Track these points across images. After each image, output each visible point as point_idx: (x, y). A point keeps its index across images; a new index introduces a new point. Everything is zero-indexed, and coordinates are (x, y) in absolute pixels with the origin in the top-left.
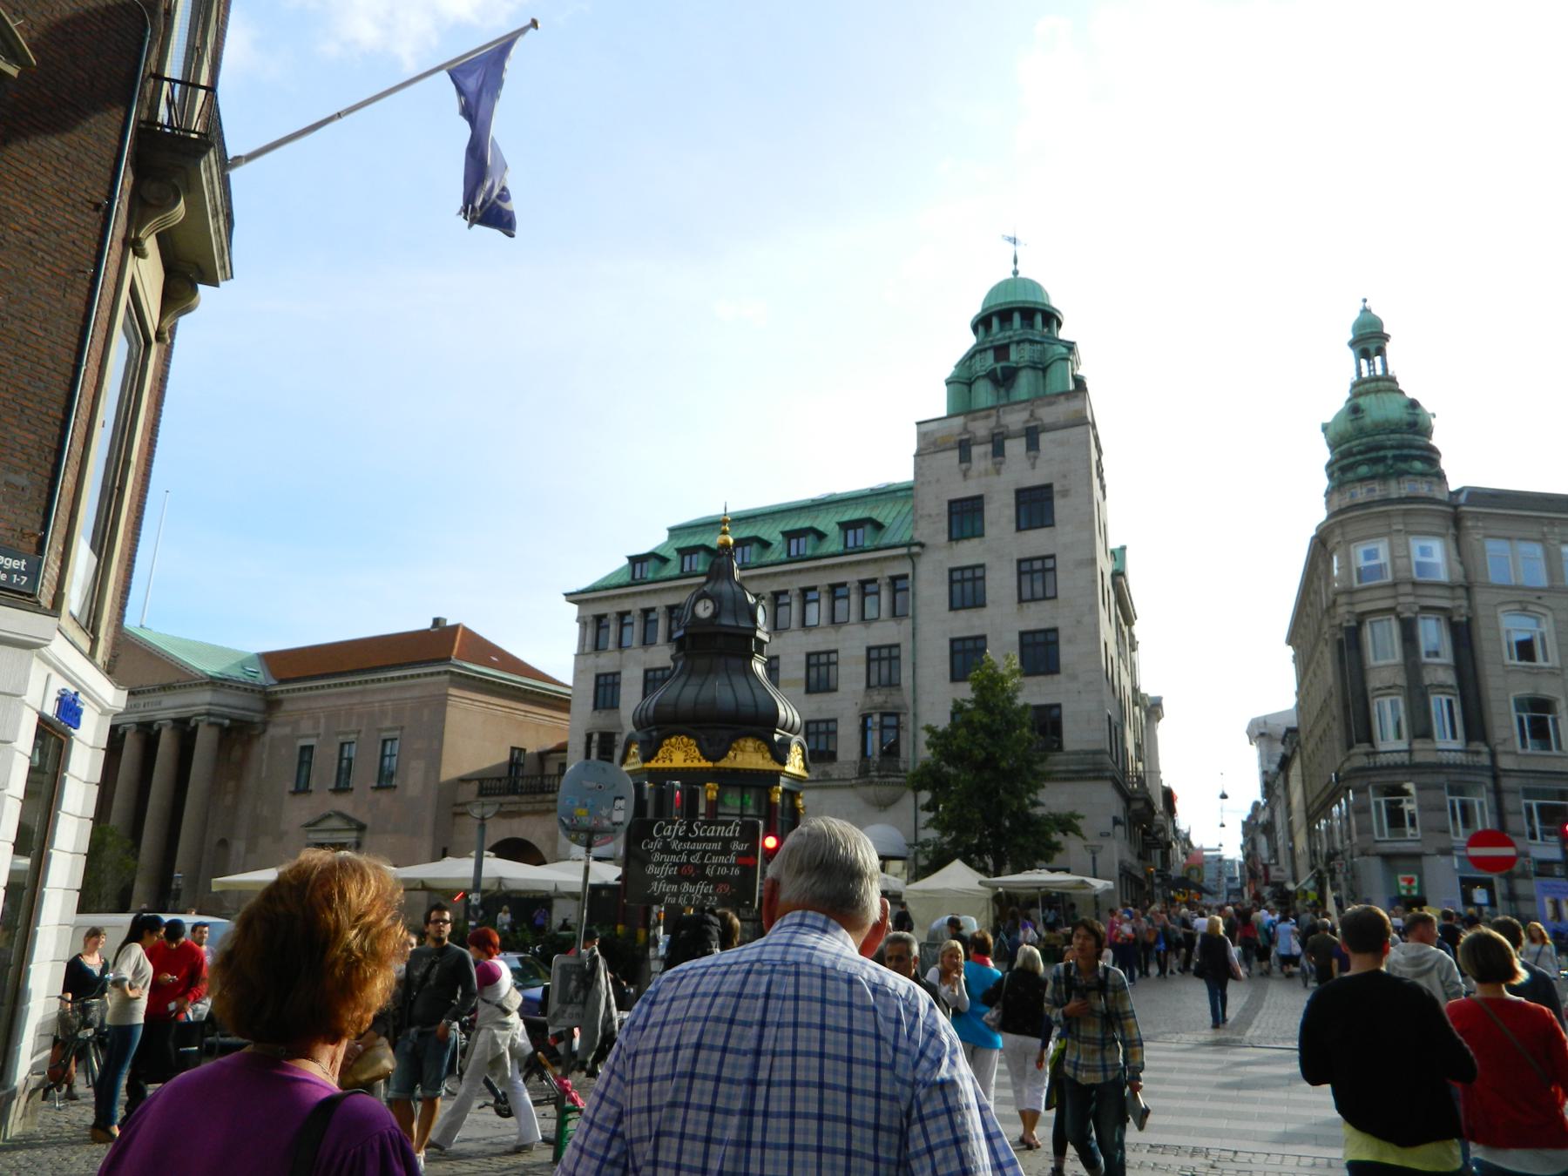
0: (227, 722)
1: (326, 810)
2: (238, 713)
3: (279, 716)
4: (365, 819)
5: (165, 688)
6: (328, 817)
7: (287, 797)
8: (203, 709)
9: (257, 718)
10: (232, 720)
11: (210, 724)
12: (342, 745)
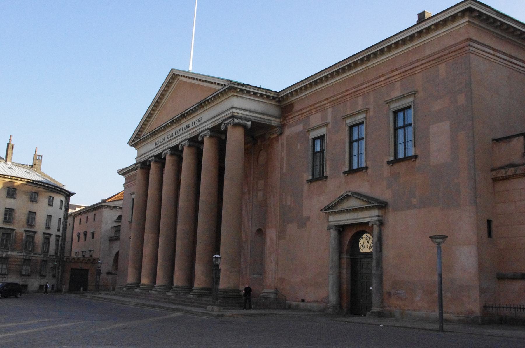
0: (249, 123)
1: (343, 192)
2: (258, 117)
4: (385, 195)
5: (202, 104)
6: (346, 197)
7: (306, 186)
8: (228, 114)
9: (275, 122)
10: (252, 122)
11: (236, 125)
12: (351, 128)
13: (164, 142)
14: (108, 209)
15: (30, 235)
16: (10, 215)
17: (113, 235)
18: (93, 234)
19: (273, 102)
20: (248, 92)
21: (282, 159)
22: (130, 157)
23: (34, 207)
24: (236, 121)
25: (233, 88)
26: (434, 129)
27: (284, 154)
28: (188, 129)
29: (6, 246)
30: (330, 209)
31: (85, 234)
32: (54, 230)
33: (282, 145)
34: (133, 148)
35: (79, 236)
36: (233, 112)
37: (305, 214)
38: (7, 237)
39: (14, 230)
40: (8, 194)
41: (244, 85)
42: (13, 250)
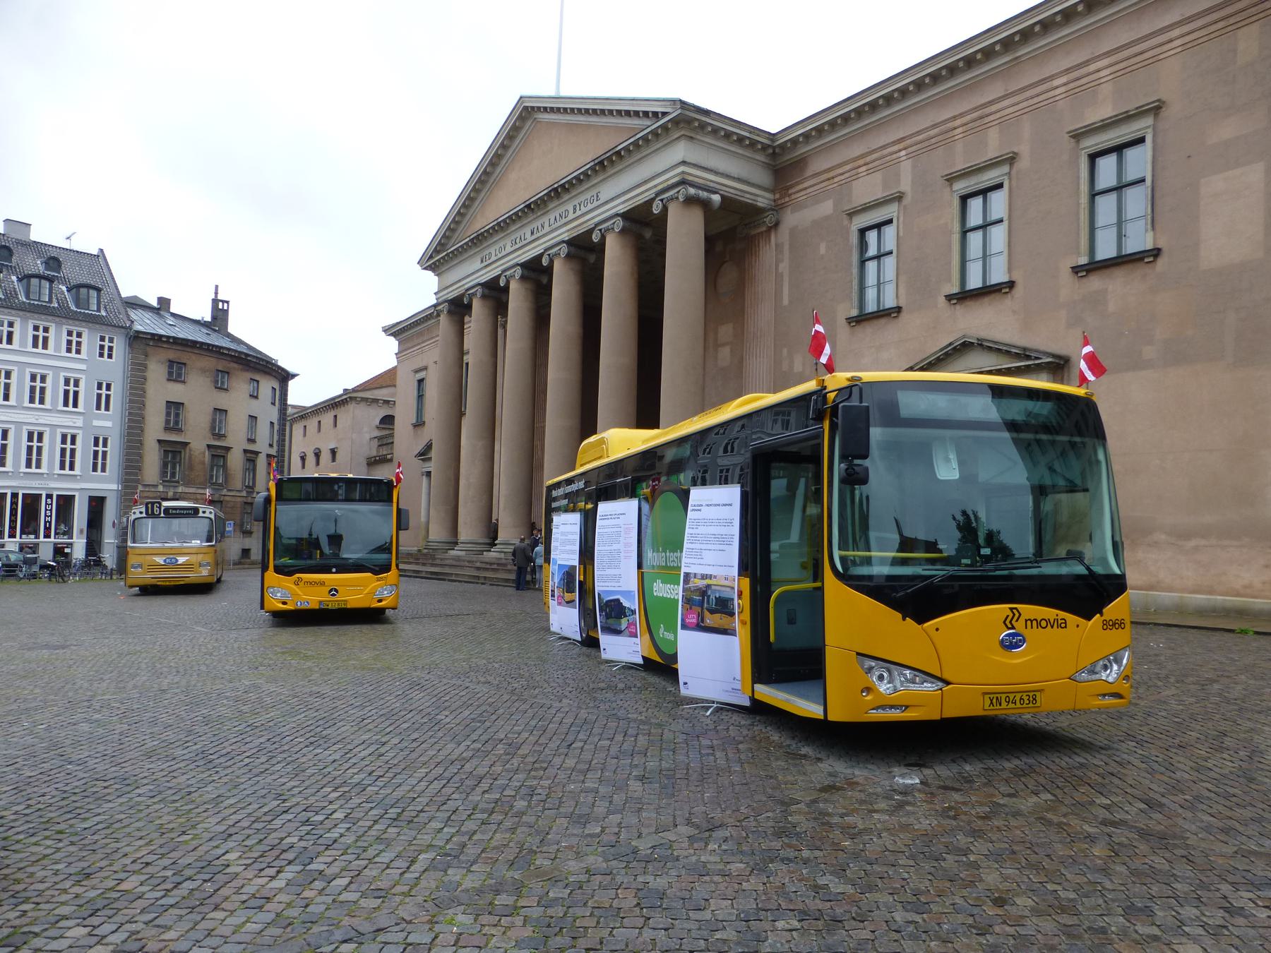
0: (716, 198)
2: (733, 188)
3: (805, 189)
5: (604, 165)
8: (672, 177)
10: (722, 196)
11: (690, 201)
13: (504, 253)
14: (363, 404)
15: (219, 454)
16: (177, 415)
17: (374, 453)
18: (333, 452)
19: (761, 157)
20: (715, 131)
21: (779, 277)
22: (423, 291)
23: (222, 400)
24: (692, 191)
25: (689, 121)
26: (1214, 184)
27: (784, 267)
28: (564, 221)
29: (173, 475)
31: (317, 455)
32: (263, 445)
33: (779, 247)
34: (430, 274)
35: (303, 459)
36: (683, 172)
38: (174, 458)
39: (186, 444)
40: (170, 373)
41: (707, 113)
42: (187, 484)
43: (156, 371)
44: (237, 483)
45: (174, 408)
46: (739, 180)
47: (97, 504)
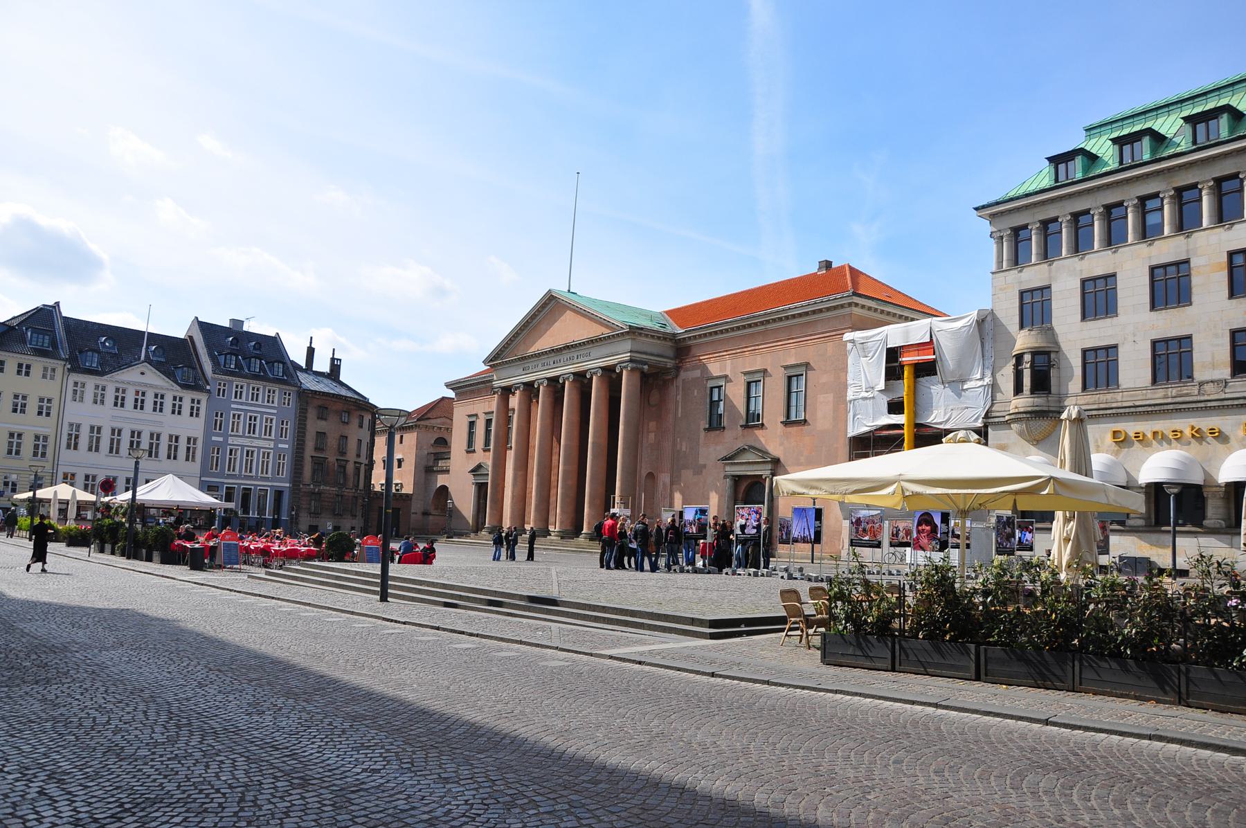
1: (740, 445)
6: (742, 451)
7: (702, 434)
9: (670, 364)
12: (749, 384)
15: (343, 467)
19: (670, 344)
21: (677, 402)
26: (821, 398)
27: (679, 398)
30: (729, 459)
37: (701, 461)
43: (312, 414)
44: (351, 484)
45: (321, 435)
46: (658, 356)
47: (279, 494)
